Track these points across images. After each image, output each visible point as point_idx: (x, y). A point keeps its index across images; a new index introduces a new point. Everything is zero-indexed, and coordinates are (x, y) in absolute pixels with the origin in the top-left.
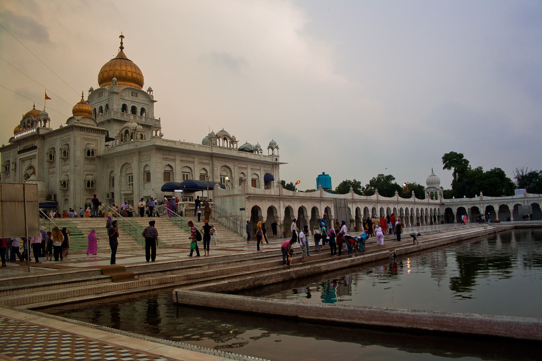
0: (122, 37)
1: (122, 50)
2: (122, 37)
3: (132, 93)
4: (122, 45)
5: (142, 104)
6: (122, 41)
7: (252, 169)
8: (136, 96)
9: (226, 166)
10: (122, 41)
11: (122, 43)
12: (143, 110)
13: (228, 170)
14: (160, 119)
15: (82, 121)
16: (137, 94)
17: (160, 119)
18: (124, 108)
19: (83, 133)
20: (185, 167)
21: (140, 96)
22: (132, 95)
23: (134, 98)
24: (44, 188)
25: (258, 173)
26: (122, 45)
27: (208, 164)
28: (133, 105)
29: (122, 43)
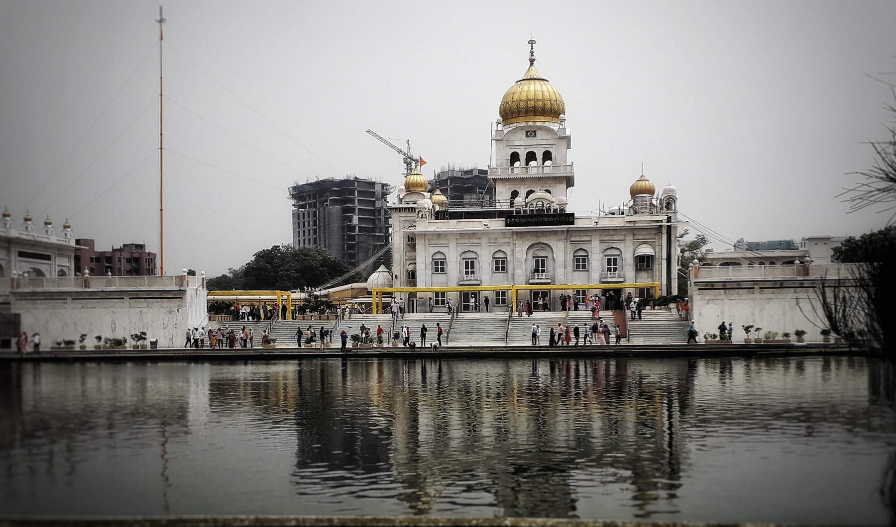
0: (532, 42)
1: (532, 64)
2: (532, 42)
3: (527, 132)
4: (532, 55)
5: (544, 146)
6: (532, 47)
7: (602, 241)
8: (535, 136)
9: (539, 243)
10: (532, 47)
11: (532, 53)
12: (547, 156)
13: (548, 249)
14: (572, 163)
15: (408, 199)
16: (535, 132)
17: (572, 163)
18: (515, 157)
19: (403, 214)
20: (466, 252)
21: (539, 133)
22: (527, 136)
23: (531, 141)
24: (386, 281)
25: (620, 246)
26: (532, 55)
27: (508, 244)
28: (529, 150)
29: (532, 53)
